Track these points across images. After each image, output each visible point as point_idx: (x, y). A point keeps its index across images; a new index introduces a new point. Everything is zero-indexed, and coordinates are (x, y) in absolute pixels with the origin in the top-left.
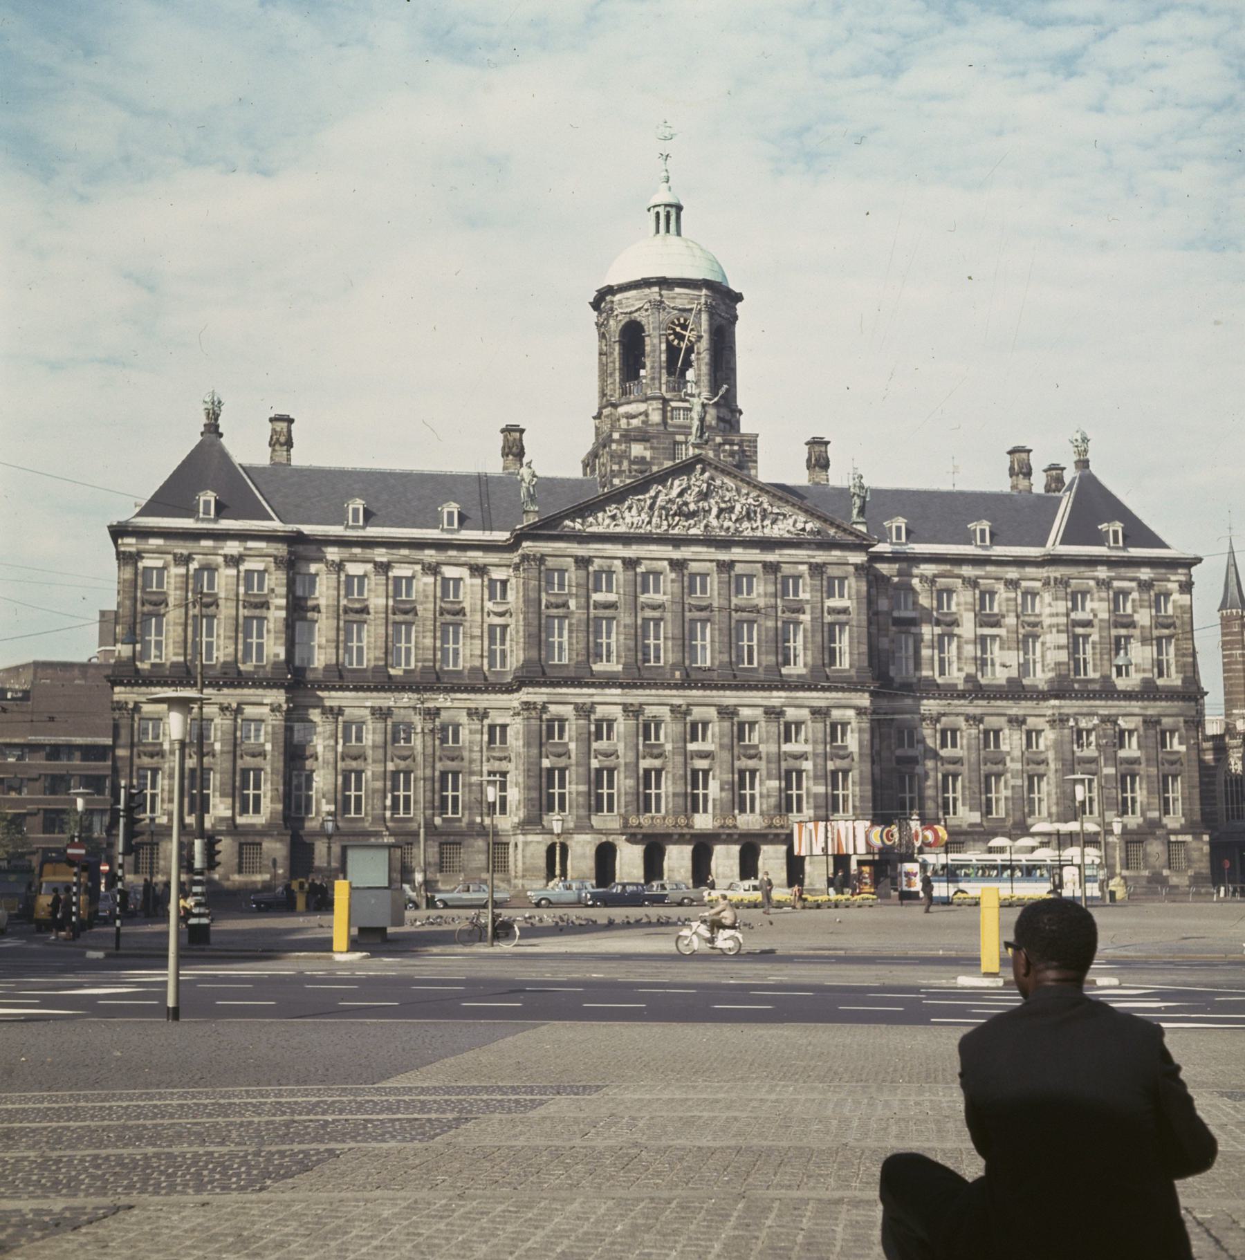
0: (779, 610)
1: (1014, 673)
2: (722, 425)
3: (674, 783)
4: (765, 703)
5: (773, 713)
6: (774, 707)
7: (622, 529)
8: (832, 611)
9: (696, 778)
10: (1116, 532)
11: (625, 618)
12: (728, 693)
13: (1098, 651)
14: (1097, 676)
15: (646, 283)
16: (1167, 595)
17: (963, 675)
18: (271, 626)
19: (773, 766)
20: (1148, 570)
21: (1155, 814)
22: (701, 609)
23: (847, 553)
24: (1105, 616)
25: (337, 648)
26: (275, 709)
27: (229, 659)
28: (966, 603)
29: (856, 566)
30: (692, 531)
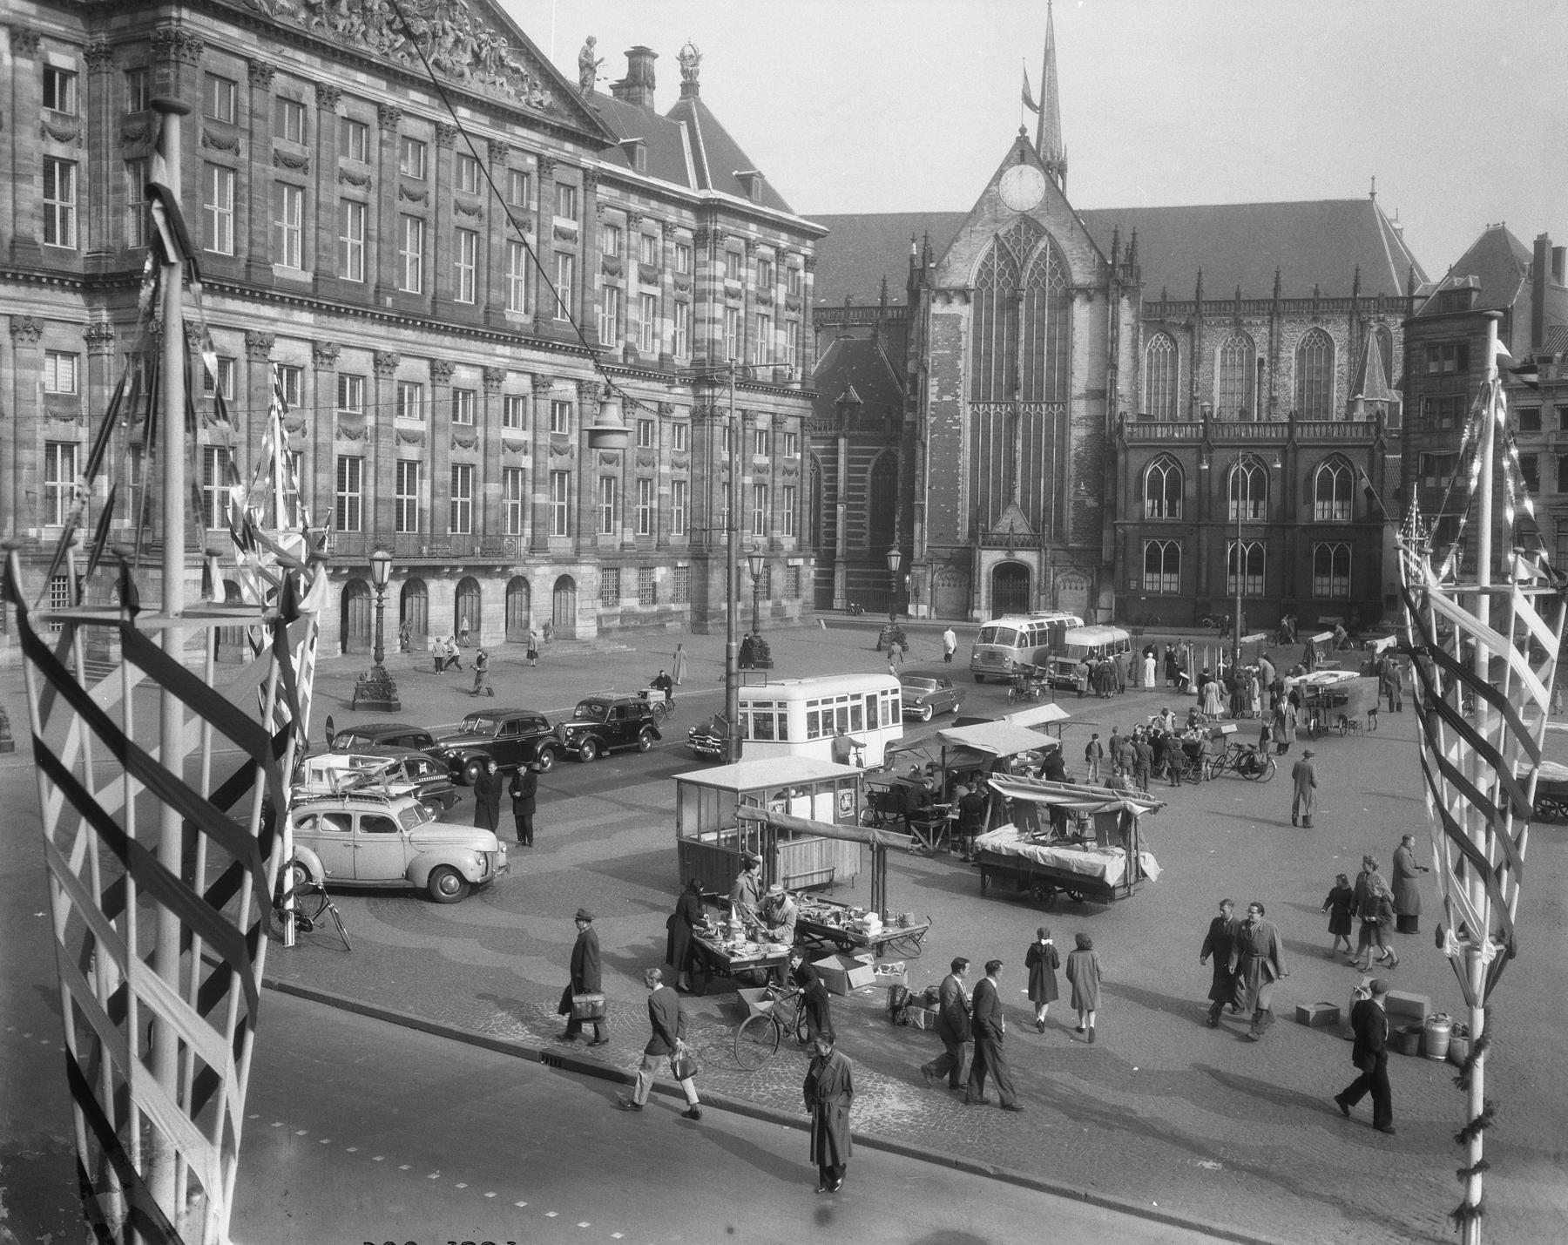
1: (668, 350)
4: (487, 362)
5: (491, 377)
6: (497, 370)
8: (561, 234)
9: (407, 472)
12: (448, 340)
14: (741, 361)
16: (795, 269)
17: (622, 343)
20: (784, 236)
21: (777, 534)
22: (414, 198)
23: (580, 150)
24: (751, 287)
29: (585, 170)
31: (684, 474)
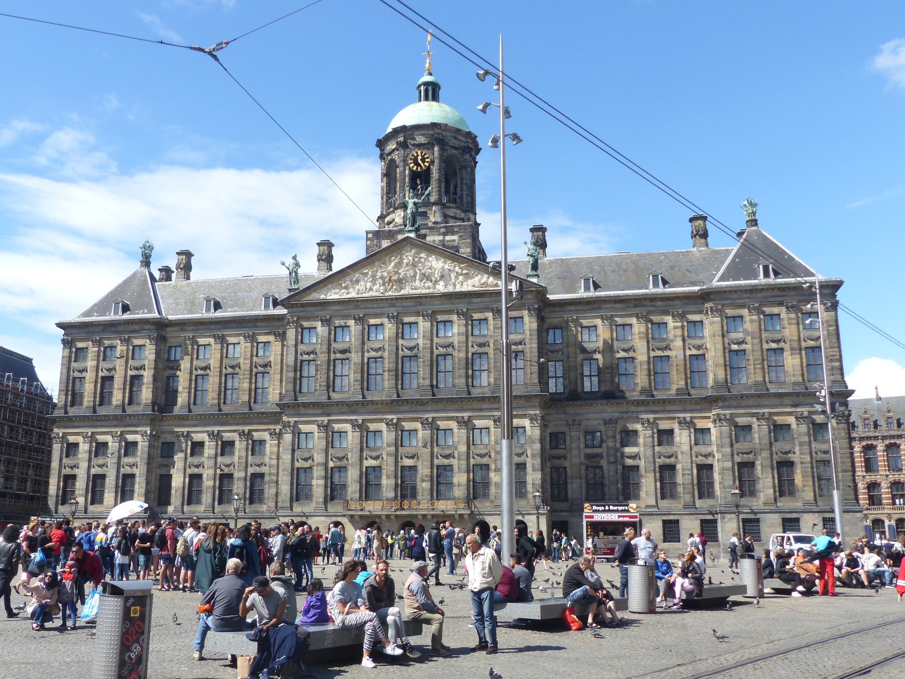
0: (470, 344)
2: (450, 220)
3: (388, 477)
6: (463, 417)
7: (353, 294)
10: (766, 269)
11: (355, 357)
13: (751, 362)
15: (396, 131)
18: (145, 380)
19: (464, 462)
25: (189, 393)
26: (143, 434)
27: (119, 403)
28: (640, 333)
30: (402, 292)
31: (709, 461)
